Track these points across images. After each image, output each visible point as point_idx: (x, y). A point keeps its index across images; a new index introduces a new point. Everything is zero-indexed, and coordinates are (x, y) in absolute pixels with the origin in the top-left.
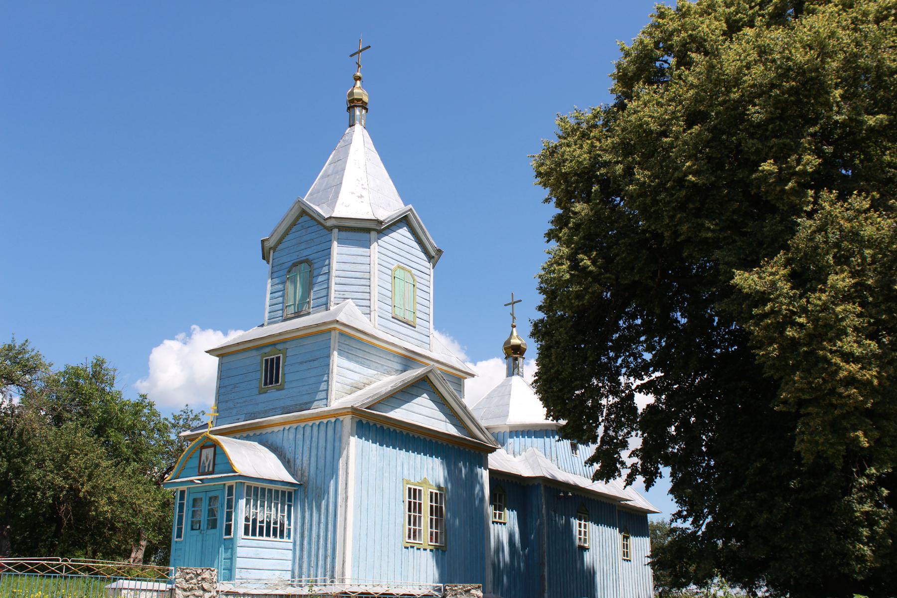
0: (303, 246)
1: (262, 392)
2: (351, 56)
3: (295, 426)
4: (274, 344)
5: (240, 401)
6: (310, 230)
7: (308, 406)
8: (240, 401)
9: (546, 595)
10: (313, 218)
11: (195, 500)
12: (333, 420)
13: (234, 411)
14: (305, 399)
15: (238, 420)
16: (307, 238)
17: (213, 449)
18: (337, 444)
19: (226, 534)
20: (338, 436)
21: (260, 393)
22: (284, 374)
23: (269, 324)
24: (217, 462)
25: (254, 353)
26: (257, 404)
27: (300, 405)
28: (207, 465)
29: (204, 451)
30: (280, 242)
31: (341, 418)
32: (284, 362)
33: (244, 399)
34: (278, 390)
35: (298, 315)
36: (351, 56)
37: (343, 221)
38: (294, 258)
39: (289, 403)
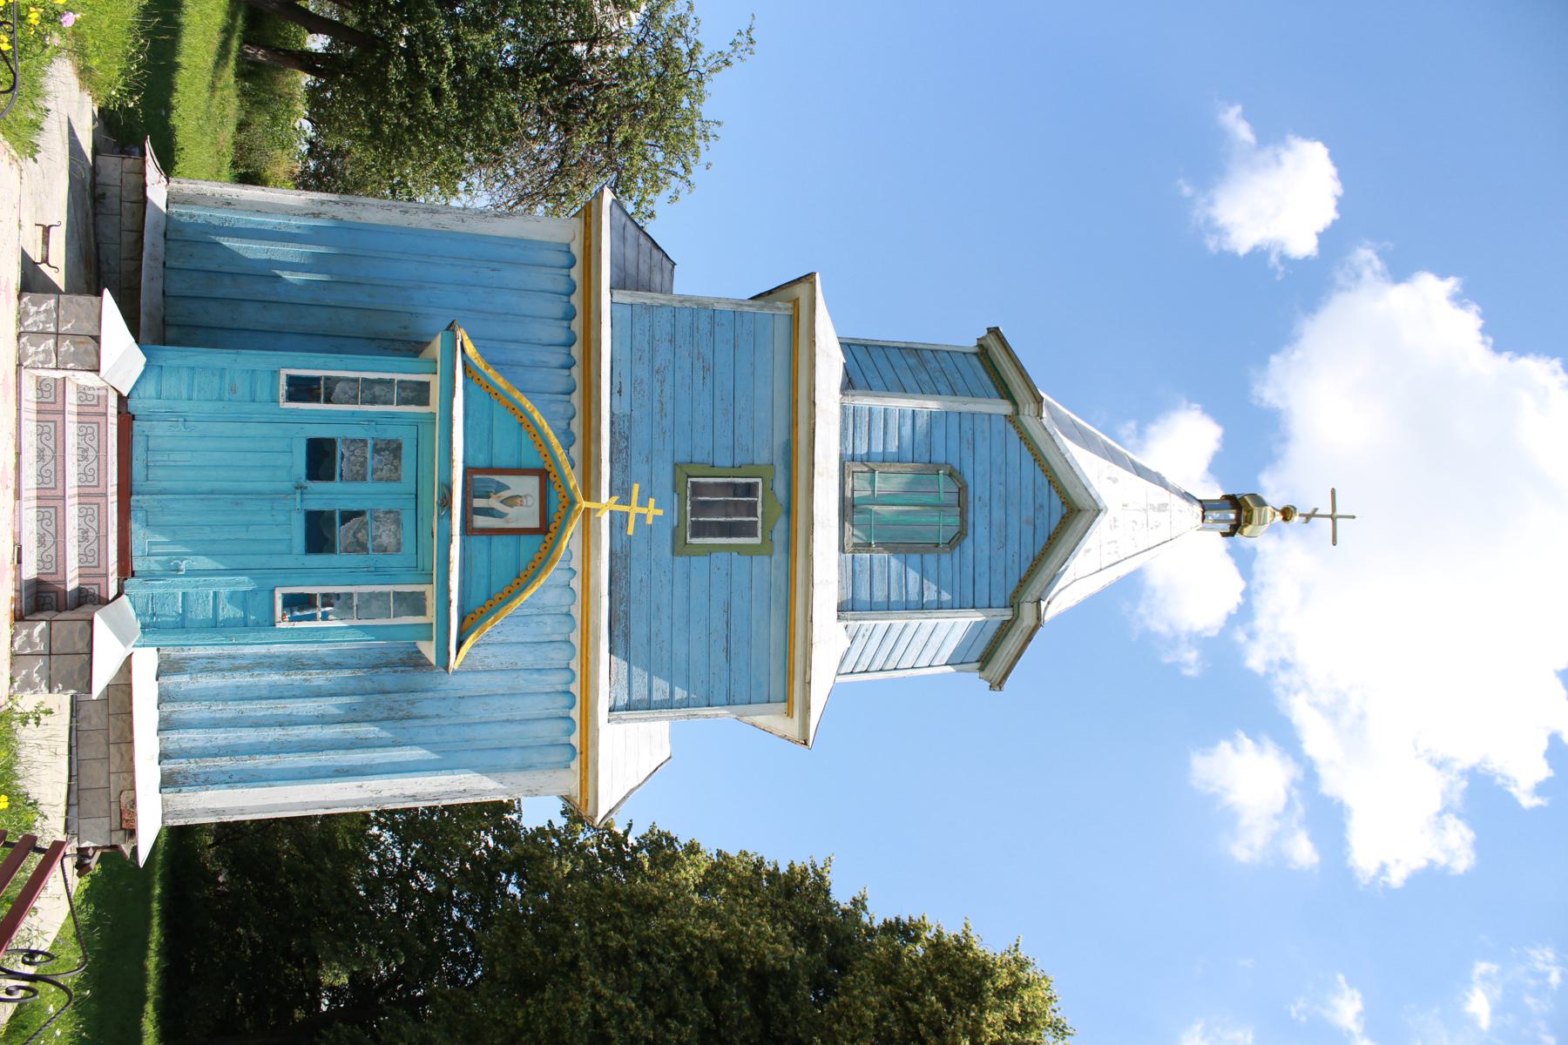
0: (998, 514)
1: (681, 470)
2: (1333, 492)
3: (576, 612)
4: (789, 511)
5: (668, 388)
6: (1028, 531)
7: (620, 642)
8: (668, 388)
9: (149, 1026)
10: (1053, 540)
11: (393, 449)
12: (575, 740)
13: (642, 372)
14: (638, 630)
15: (616, 391)
16: (1013, 532)
17: (535, 523)
18: (514, 757)
19: (292, 380)
20: (535, 757)
21: (675, 465)
22: (709, 550)
23: (843, 408)
24: (497, 540)
25: (780, 437)
26: (649, 460)
27: (627, 614)
28: (493, 503)
29: (530, 485)
30: (1025, 438)
31: (575, 765)
32: (740, 549)
33: (669, 408)
34: (675, 531)
35: (848, 509)
36: (1333, 492)
37: (1022, 638)
38: (979, 488)
39: (637, 572)
